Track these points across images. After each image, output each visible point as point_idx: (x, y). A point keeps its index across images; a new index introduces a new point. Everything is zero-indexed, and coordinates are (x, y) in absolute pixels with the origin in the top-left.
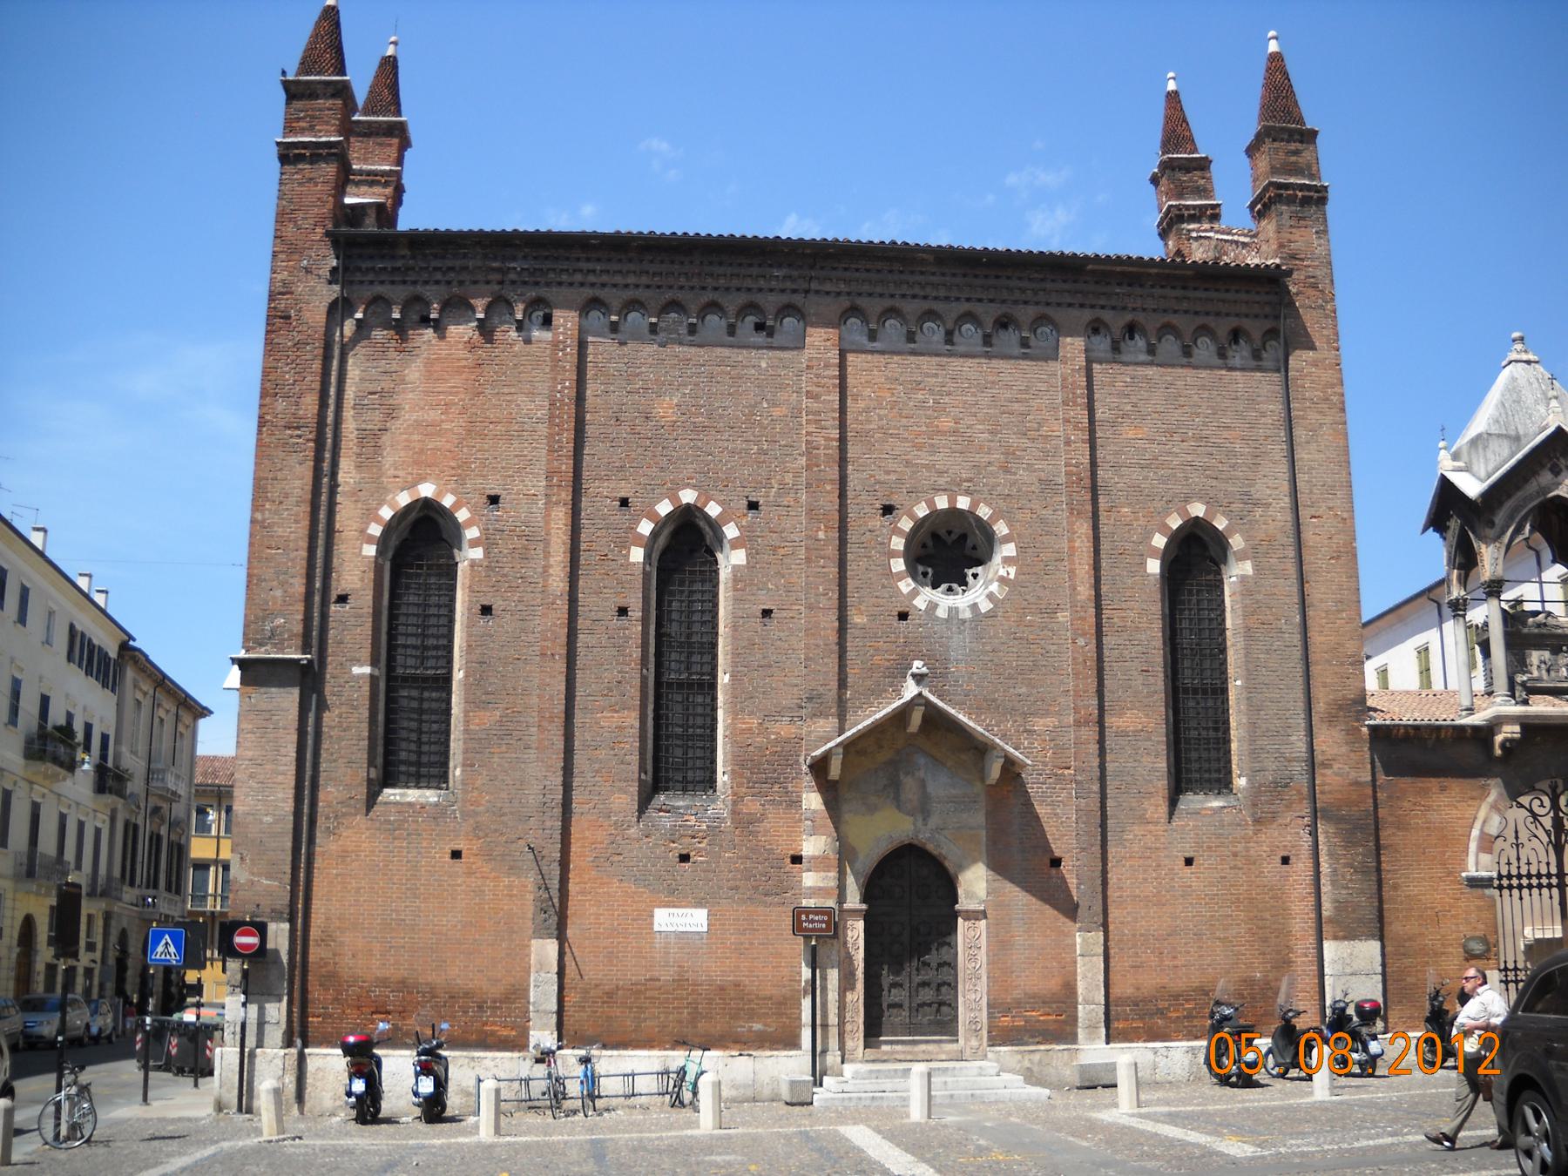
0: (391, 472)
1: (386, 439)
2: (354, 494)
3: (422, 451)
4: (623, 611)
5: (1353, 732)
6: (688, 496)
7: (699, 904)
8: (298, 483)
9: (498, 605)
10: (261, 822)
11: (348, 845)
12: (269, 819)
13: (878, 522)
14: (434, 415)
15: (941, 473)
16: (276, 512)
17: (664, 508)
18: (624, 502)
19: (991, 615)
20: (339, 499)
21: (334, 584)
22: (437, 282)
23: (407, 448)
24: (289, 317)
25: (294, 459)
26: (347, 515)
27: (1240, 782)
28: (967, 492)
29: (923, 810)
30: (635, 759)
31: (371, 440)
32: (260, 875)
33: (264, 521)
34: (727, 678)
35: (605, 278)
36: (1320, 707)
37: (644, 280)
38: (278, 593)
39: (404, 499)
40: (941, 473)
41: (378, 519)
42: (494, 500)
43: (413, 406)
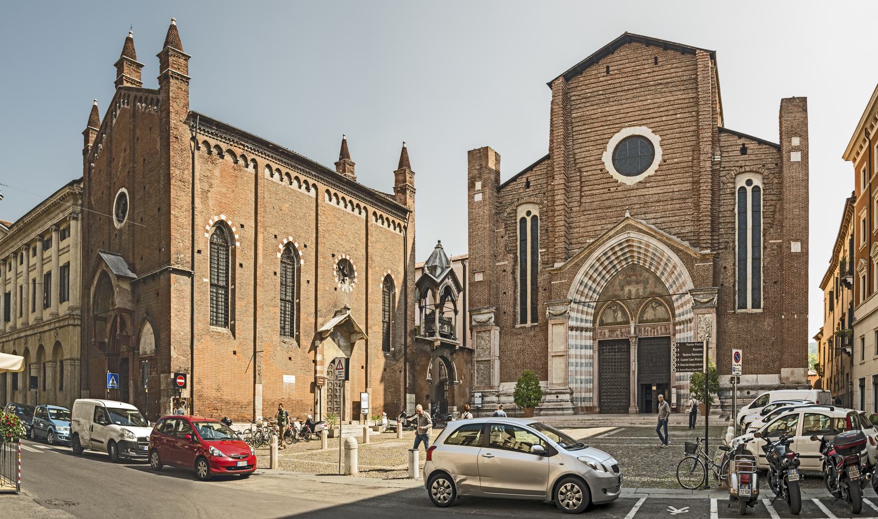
4: (275, 273)
6: (291, 239)
9: (244, 264)
13: (331, 258)
17: (285, 241)
18: (276, 236)
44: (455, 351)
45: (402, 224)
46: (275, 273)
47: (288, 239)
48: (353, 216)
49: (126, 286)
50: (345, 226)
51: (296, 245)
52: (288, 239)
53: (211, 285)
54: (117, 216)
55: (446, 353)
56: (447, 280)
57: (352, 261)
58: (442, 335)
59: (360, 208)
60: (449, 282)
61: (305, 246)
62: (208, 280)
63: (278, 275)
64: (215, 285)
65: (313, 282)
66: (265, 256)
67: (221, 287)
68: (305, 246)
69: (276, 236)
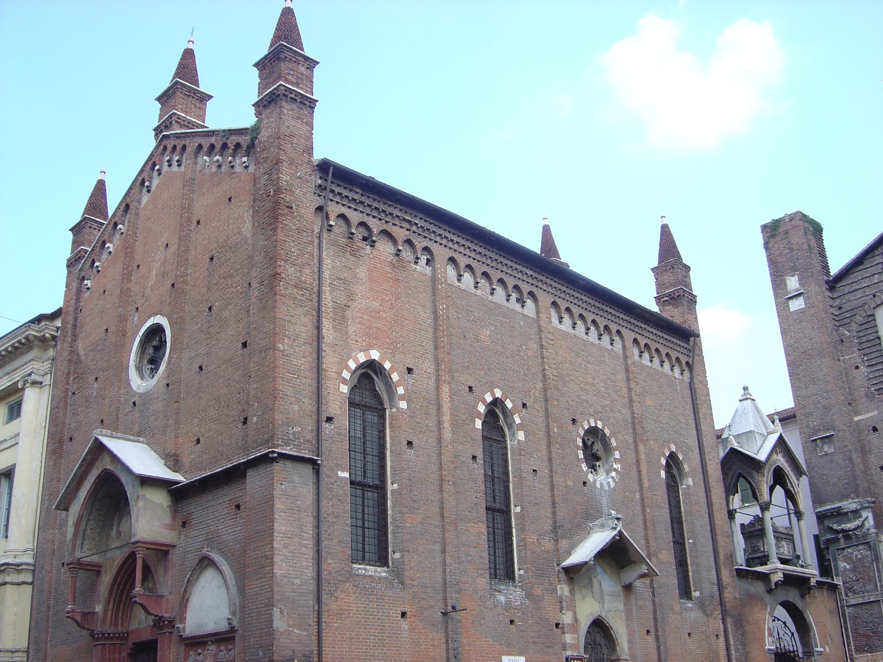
0: (353, 337)
1: (349, 312)
2: (333, 346)
3: (370, 327)
4: (474, 457)
5: (730, 571)
6: (498, 394)
7: (520, 654)
8: (303, 329)
9: (415, 442)
10: (293, 584)
11: (343, 601)
12: (297, 581)
13: (571, 427)
14: (376, 305)
15: (591, 406)
16: (291, 347)
17: (489, 398)
18: (470, 388)
19: (614, 490)
20: (324, 347)
21: (324, 407)
22: (374, 217)
23: (361, 323)
24: (291, 208)
25: (300, 311)
26: (329, 361)
27: (696, 594)
28: (601, 420)
29: (602, 601)
30: (486, 555)
31: (341, 310)
32: (293, 626)
33: (284, 351)
34: (518, 509)
35: (456, 247)
36: (721, 557)
37: (473, 254)
38: (296, 407)
39: (362, 358)
40: (591, 406)
41: (348, 369)
42: (410, 370)
43: (364, 299)
44: (810, 588)
45: (684, 360)
46: (474, 457)
47: (493, 394)
48: (601, 348)
49: (160, 498)
50: (594, 366)
51: (509, 404)
52: (493, 394)
53: (352, 483)
54: (139, 369)
55: (793, 596)
56: (774, 456)
57: (607, 432)
58: (783, 561)
59: (610, 333)
60: (780, 460)
61: (524, 405)
62: (347, 475)
63: (480, 461)
64: (359, 484)
65: (544, 472)
66: (454, 425)
67: (370, 486)
68: (524, 405)
69: (470, 388)
